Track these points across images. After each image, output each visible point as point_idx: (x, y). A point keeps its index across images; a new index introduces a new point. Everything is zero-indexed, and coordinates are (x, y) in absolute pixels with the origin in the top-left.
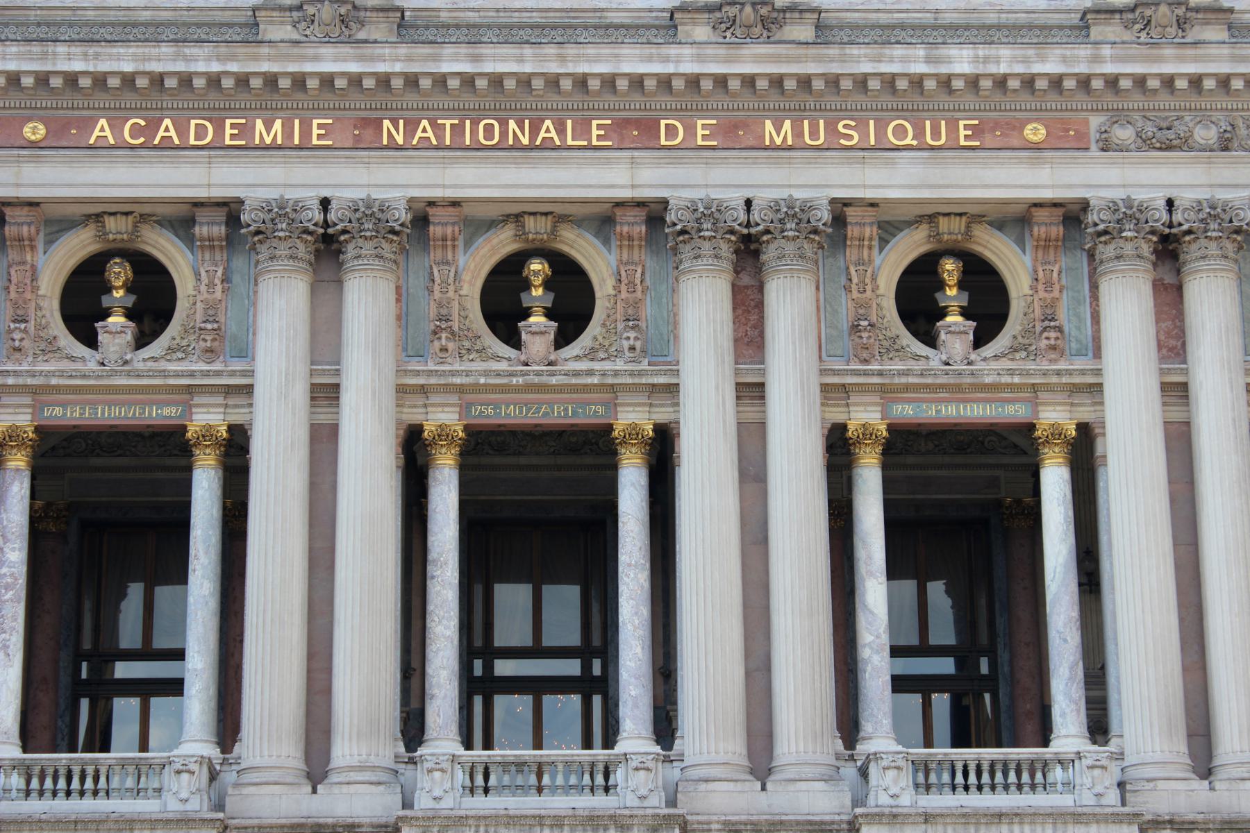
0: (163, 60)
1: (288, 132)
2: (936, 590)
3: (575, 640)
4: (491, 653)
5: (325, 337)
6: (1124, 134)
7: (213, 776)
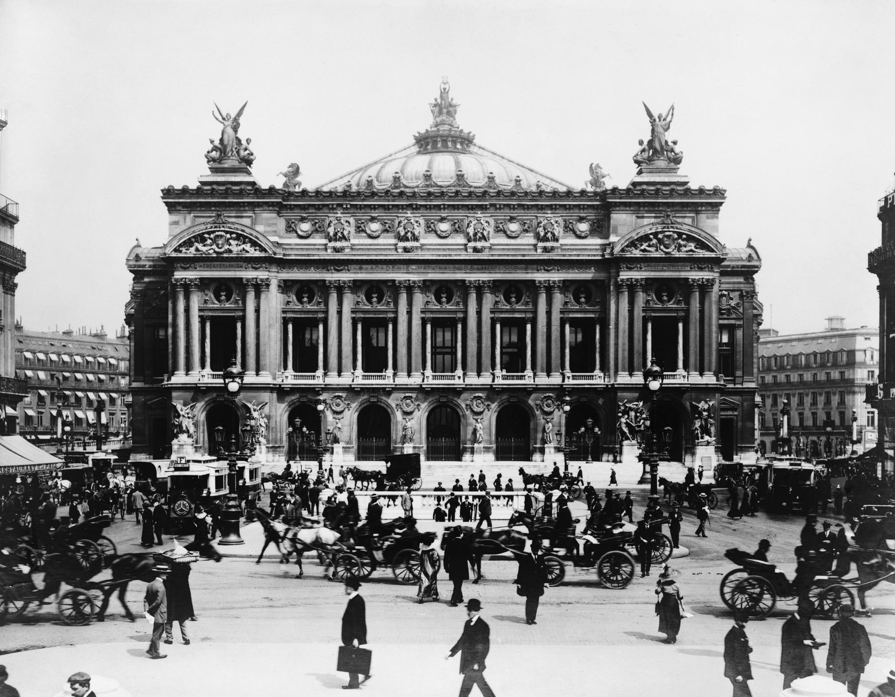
3: (450, 345)
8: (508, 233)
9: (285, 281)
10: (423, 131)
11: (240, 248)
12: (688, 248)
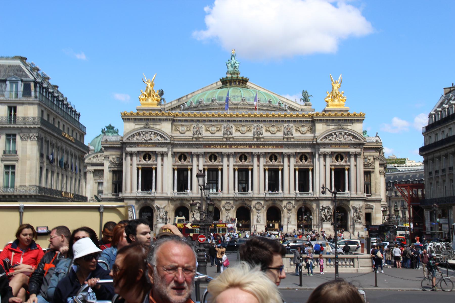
2: (273, 174)
8: (271, 131)
9: (174, 152)
10: (224, 77)
11: (156, 138)
12: (349, 139)
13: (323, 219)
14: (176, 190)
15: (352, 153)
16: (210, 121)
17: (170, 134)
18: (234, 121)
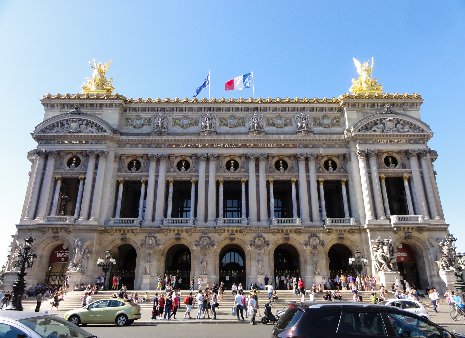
0: (189, 137)
1: (203, 146)
2: (279, 201)
3: (237, 206)
4: (227, 207)
5: (207, 170)
6: (301, 146)
7: (194, 221)
11: (88, 130)
13: (381, 264)
14: (118, 217)
15: (414, 151)
16: (181, 110)
17: (115, 127)
18: (219, 109)
